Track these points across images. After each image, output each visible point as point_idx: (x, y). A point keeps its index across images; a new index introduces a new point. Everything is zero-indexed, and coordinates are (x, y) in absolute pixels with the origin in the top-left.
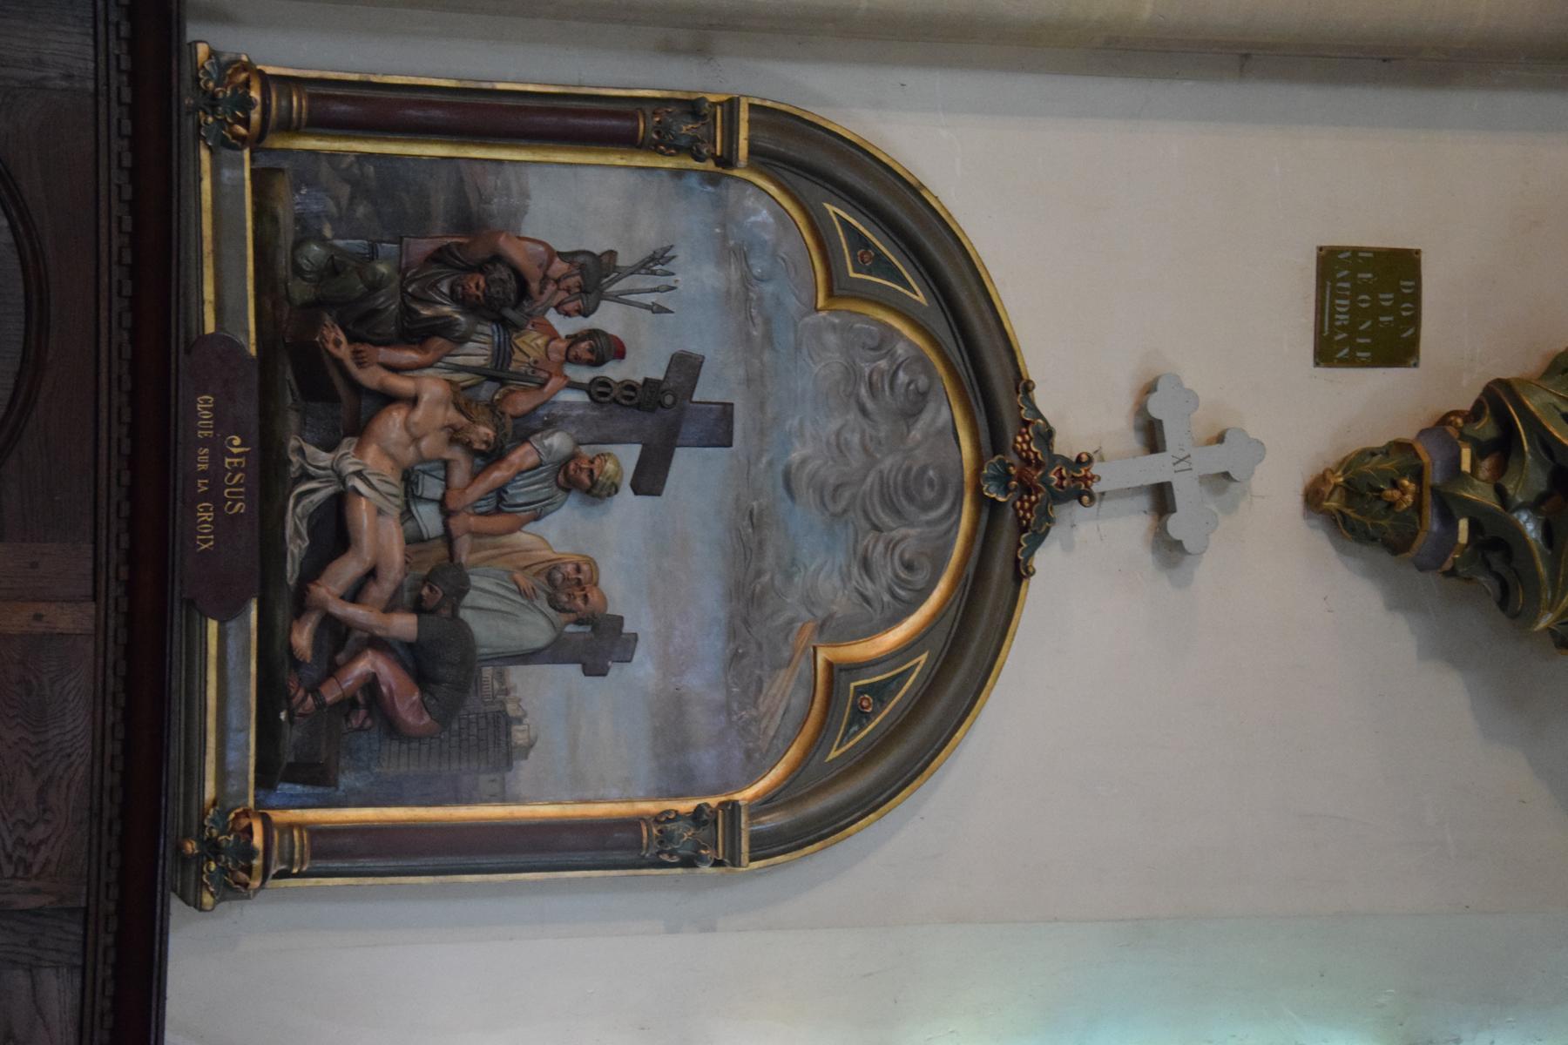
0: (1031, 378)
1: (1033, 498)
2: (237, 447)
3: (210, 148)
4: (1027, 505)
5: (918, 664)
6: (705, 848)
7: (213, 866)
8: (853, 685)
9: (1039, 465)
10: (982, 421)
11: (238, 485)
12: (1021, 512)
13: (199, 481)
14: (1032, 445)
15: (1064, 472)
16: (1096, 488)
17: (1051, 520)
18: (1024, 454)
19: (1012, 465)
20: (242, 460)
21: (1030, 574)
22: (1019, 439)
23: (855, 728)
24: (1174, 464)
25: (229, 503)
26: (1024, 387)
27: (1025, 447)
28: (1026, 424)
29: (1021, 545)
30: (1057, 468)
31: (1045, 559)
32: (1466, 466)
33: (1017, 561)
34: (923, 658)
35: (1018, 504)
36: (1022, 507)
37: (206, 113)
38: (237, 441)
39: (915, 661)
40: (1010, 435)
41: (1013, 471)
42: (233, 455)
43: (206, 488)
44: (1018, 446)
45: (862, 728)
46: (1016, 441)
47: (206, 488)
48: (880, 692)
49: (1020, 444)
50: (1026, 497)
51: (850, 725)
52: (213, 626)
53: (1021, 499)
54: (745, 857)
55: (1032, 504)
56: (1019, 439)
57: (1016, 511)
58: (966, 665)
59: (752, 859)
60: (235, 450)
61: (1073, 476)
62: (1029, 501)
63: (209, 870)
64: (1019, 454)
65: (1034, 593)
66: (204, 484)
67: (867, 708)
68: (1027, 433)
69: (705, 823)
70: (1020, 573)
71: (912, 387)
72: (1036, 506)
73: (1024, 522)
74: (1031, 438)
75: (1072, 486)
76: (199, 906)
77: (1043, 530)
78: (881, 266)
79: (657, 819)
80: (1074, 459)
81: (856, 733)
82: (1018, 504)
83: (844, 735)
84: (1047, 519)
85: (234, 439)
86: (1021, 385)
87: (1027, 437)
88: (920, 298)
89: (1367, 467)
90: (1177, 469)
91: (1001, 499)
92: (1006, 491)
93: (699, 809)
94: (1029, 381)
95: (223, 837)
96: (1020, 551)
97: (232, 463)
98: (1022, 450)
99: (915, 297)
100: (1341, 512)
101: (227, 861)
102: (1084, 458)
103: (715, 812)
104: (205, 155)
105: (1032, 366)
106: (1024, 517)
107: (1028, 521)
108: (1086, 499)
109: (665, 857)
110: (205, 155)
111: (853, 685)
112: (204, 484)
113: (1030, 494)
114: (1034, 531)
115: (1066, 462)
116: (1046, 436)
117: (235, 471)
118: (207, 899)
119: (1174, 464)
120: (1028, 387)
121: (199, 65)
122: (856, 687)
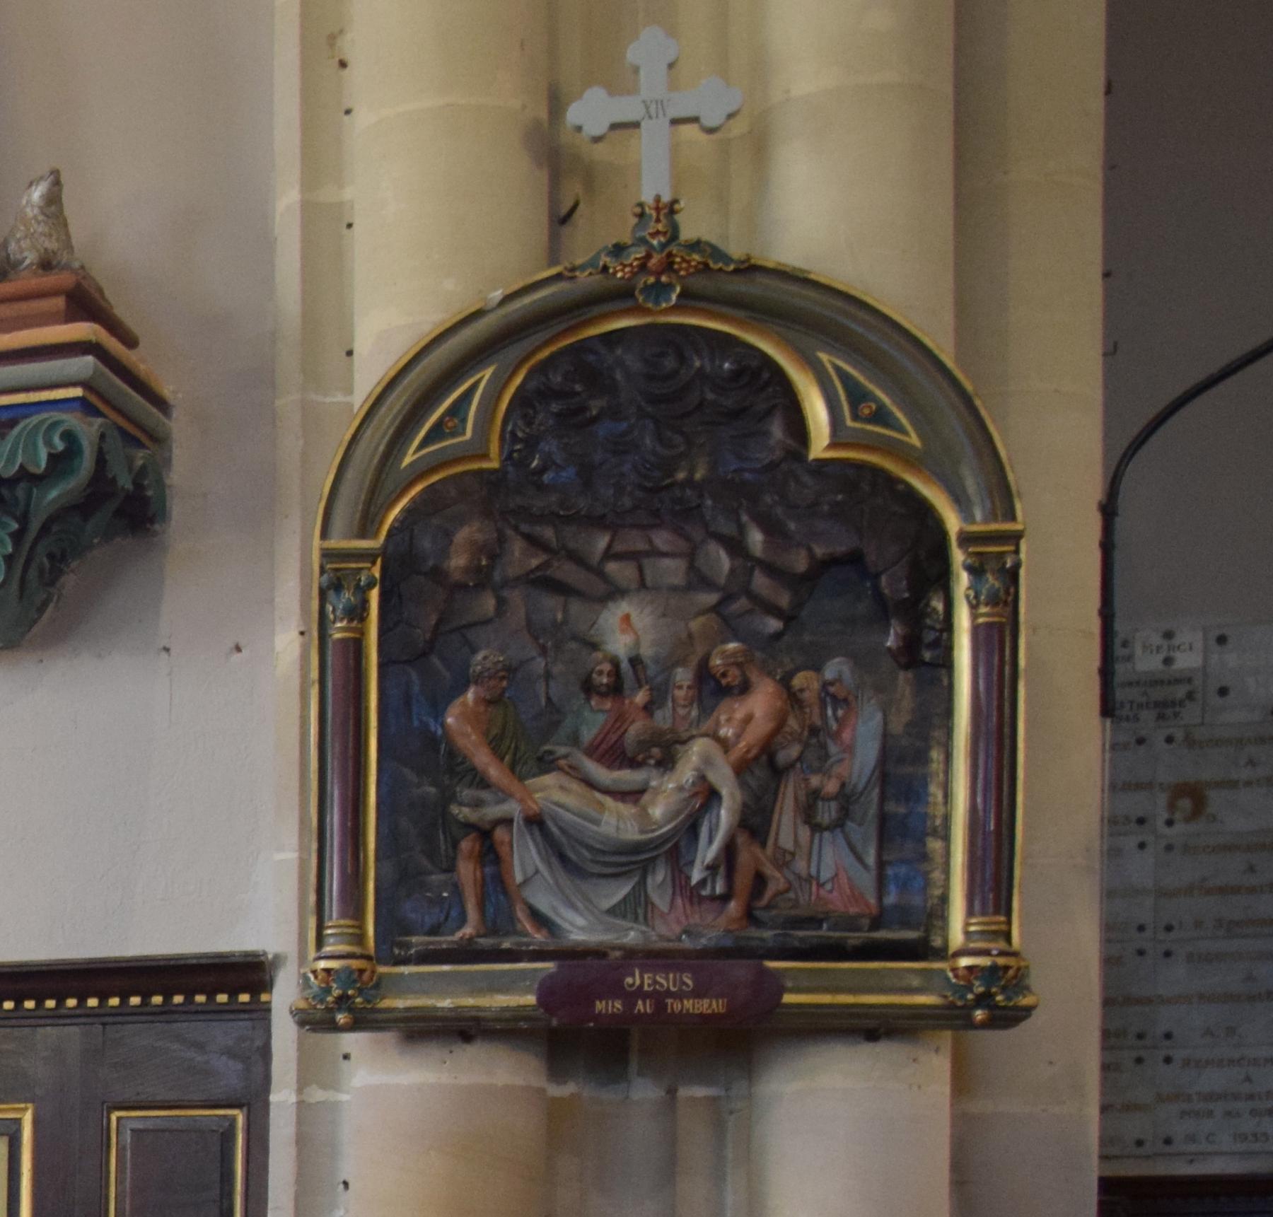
4: (684, 265)
6: (1005, 563)
9: (648, 256)
11: (667, 979)
16: (666, 198)
20: (646, 976)
21: (749, 258)
27: (627, 270)
33: (736, 271)
35: (682, 273)
36: (686, 270)
38: (629, 980)
41: (652, 280)
44: (627, 276)
49: (625, 274)
55: (684, 260)
59: (1013, 518)
60: (638, 982)
62: (680, 263)
69: (982, 565)
70: (749, 269)
78: (458, 409)
79: (973, 607)
85: (627, 984)
88: (488, 373)
91: (678, 289)
92: (669, 287)
93: (970, 569)
98: (631, 272)
99: (487, 377)
102: (638, 210)
103: (970, 555)
106: (695, 267)
109: (1010, 599)
117: (655, 982)
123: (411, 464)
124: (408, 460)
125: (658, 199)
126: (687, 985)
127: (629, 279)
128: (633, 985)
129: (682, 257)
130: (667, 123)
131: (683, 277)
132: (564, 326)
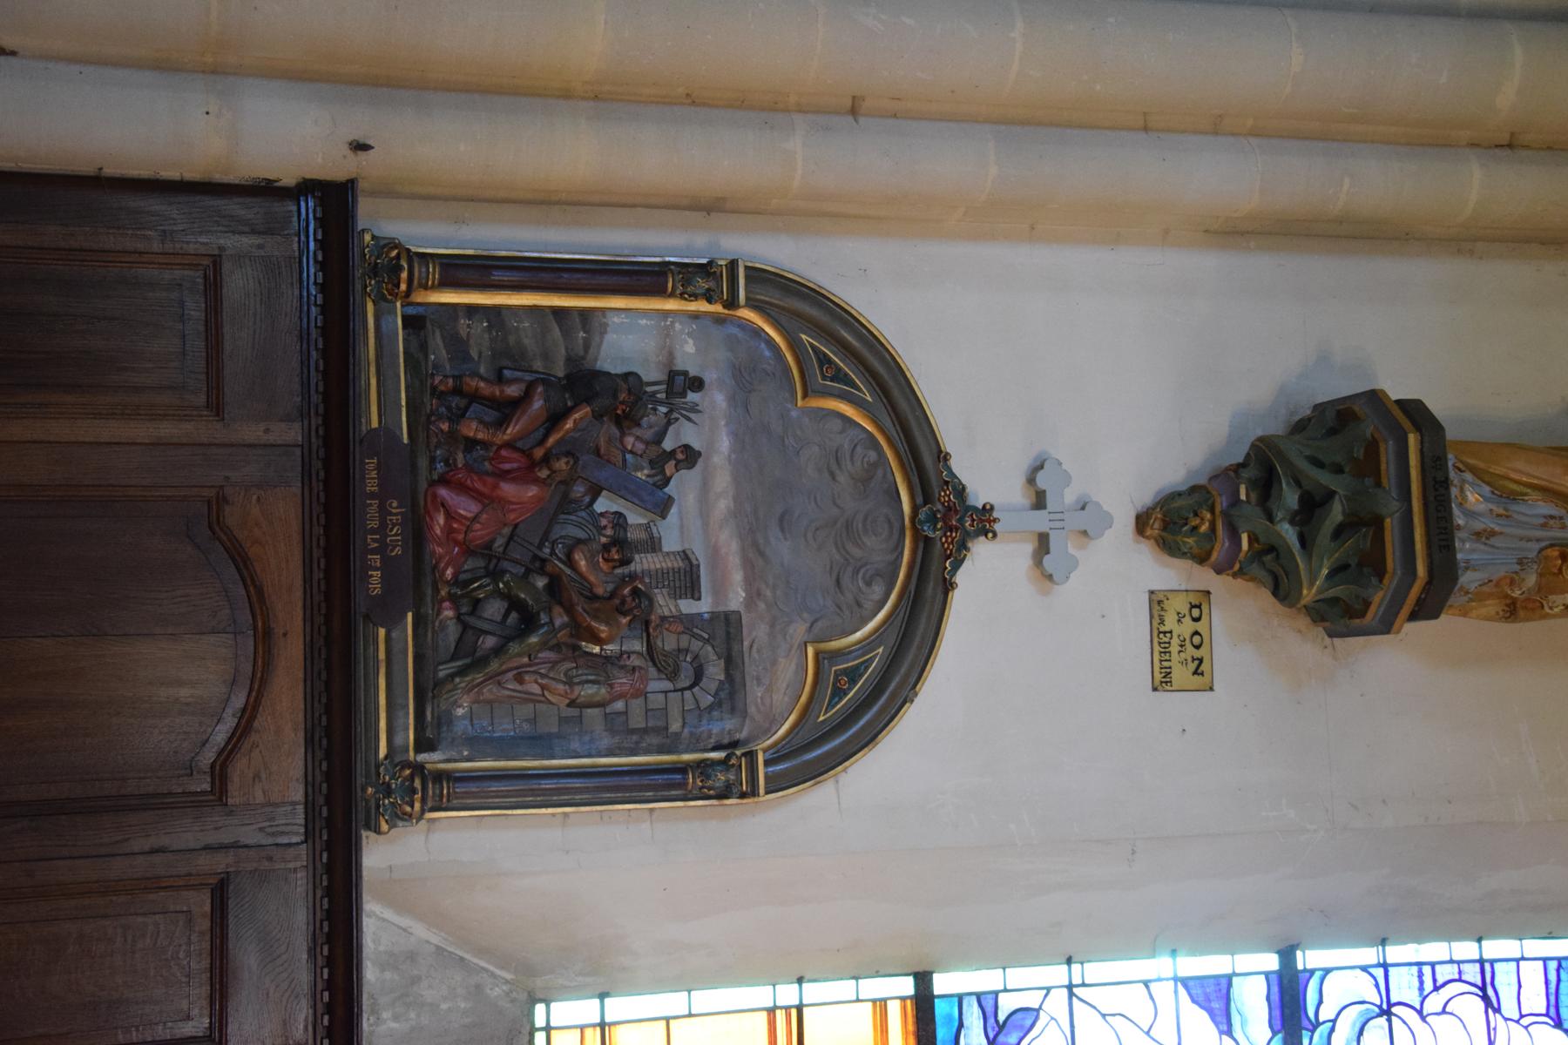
0: (948, 451)
1: (954, 534)
2: (394, 508)
3: (373, 301)
4: (950, 540)
5: (877, 654)
7: (387, 801)
8: (834, 669)
10: (916, 480)
11: (396, 535)
12: (946, 545)
13: (369, 537)
14: (951, 497)
15: (974, 517)
16: (997, 527)
17: (968, 549)
18: (946, 504)
19: (938, 511)
20: (399, 517)
22: (943, 494)
23: (837, 699)
25: (390, 548)
26: (942, 457)
28: (947, 483)
29: (946, 568)
30: (970, 513)
31: (961, 577)
32: (1243, 497)
34: (881, 650)
35: (944, 539)
36: (946, 541)
37: (370, 278)
38: (395, 504)
39: (876, 652)
40: (936, 491)
42: (391, 514)
43: (376, 545)
45: (841, 699)
46: (940, 495)
47: (376, 545)
48: (853, 675)
50: (949, 534)
51: (833, 696)
52: (382, 632)
53: (945, 535)
54: (762, 791)
56: (943, 494)
57: (943, 544)
58: (910, 657)
59: (767, 793)
60: (394, 511)
61: (981, 519)
62: (951, 536)
63: (383, 804)
64: (943, 504)
65: (959, 601)
66: (374, 540)
67: (844, 685)
68: (948, 489)
70: (948, 586)
71: (866, 459)
72: (956, 540)
73: (949, 552)
74: (950, 493)
75: (980, 526)
76: (378, 831)
77: (962, 556)
80: (981, 507)
81: (837, 703)
82: (944, 539)
83: (828, 705)
84: (963, 546)
86: (942, 456)
87: (948, 492)
89: (1179, 503)
90: (1062, 522)
92: (935, 529)
94: (947, 454)
95: (393, 781)
96: (946, 571)
97: (390, 520)
100: (1160, 536)
101: (396, 798)
102: (988, 507)
104: (370, 307)
105: (949, 443)
107: (951, 551)
108: (990, 535)
110: (370, 307)
111: (834, 669)
112: (374, 540)
113: (951, 532)
114: (957, 556)
115: (975, 508)
116: (961, 491)
118: (384, 827)
120: (947, 457)
121: (365, 245)
122: (836, 671)
123: (802, 339)
124: (804, 337)
125: (995, 520)
126: (392, 551)
127: (939, 500)
128: (390, 506)
129: (956, 537)
130: (1044, 528)
131: (941, 539)
132: (904, 455)
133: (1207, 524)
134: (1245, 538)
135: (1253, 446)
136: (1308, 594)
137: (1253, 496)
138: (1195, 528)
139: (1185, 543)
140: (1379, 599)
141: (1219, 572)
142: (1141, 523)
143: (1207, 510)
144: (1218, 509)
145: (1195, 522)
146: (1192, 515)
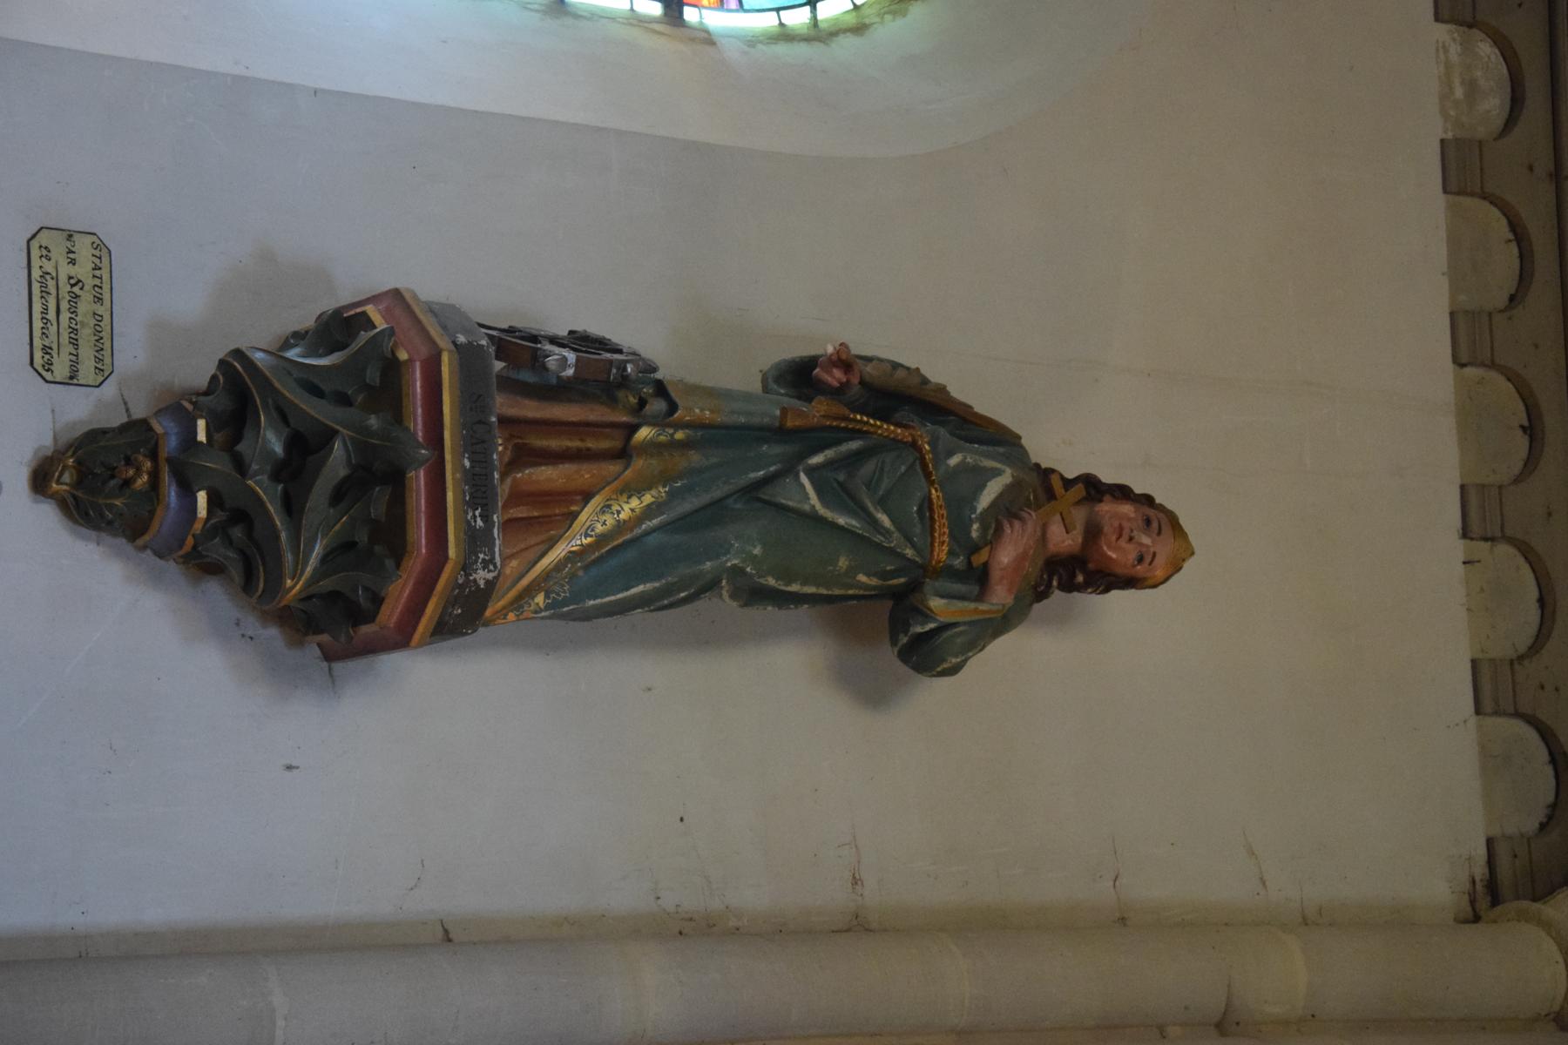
24: (473, 444)
119: (473, 444)
133: (145, 477)
134: (202, 497)
135: (223, 364)
136: (294, 587)
137: (218, 437)
138: (127, 483)
139: (111, 507)
140: (399, 592)
141: (160, 556)
142: (40, 480)
143: (145, 456)
144: (164, 453)
145: (131, 472)
146: (123, 463)
